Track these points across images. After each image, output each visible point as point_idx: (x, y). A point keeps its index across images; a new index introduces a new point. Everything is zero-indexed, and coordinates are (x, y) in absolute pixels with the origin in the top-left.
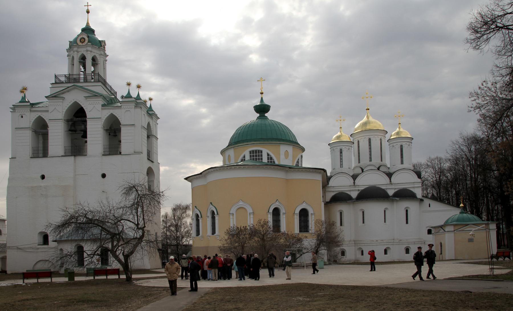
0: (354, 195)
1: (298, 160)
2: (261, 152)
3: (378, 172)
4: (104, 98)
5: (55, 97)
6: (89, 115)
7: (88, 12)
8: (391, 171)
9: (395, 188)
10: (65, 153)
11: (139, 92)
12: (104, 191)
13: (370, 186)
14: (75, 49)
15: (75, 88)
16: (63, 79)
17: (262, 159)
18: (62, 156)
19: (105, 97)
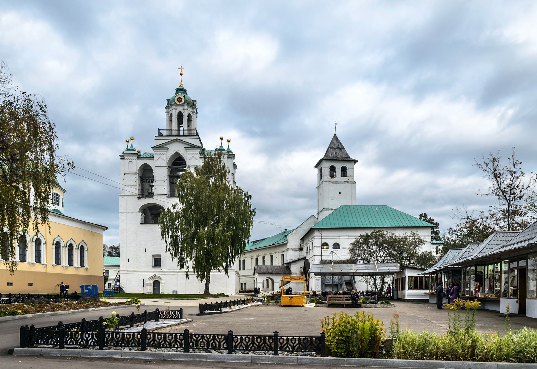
7: (181, 74)
14: (174, 107)
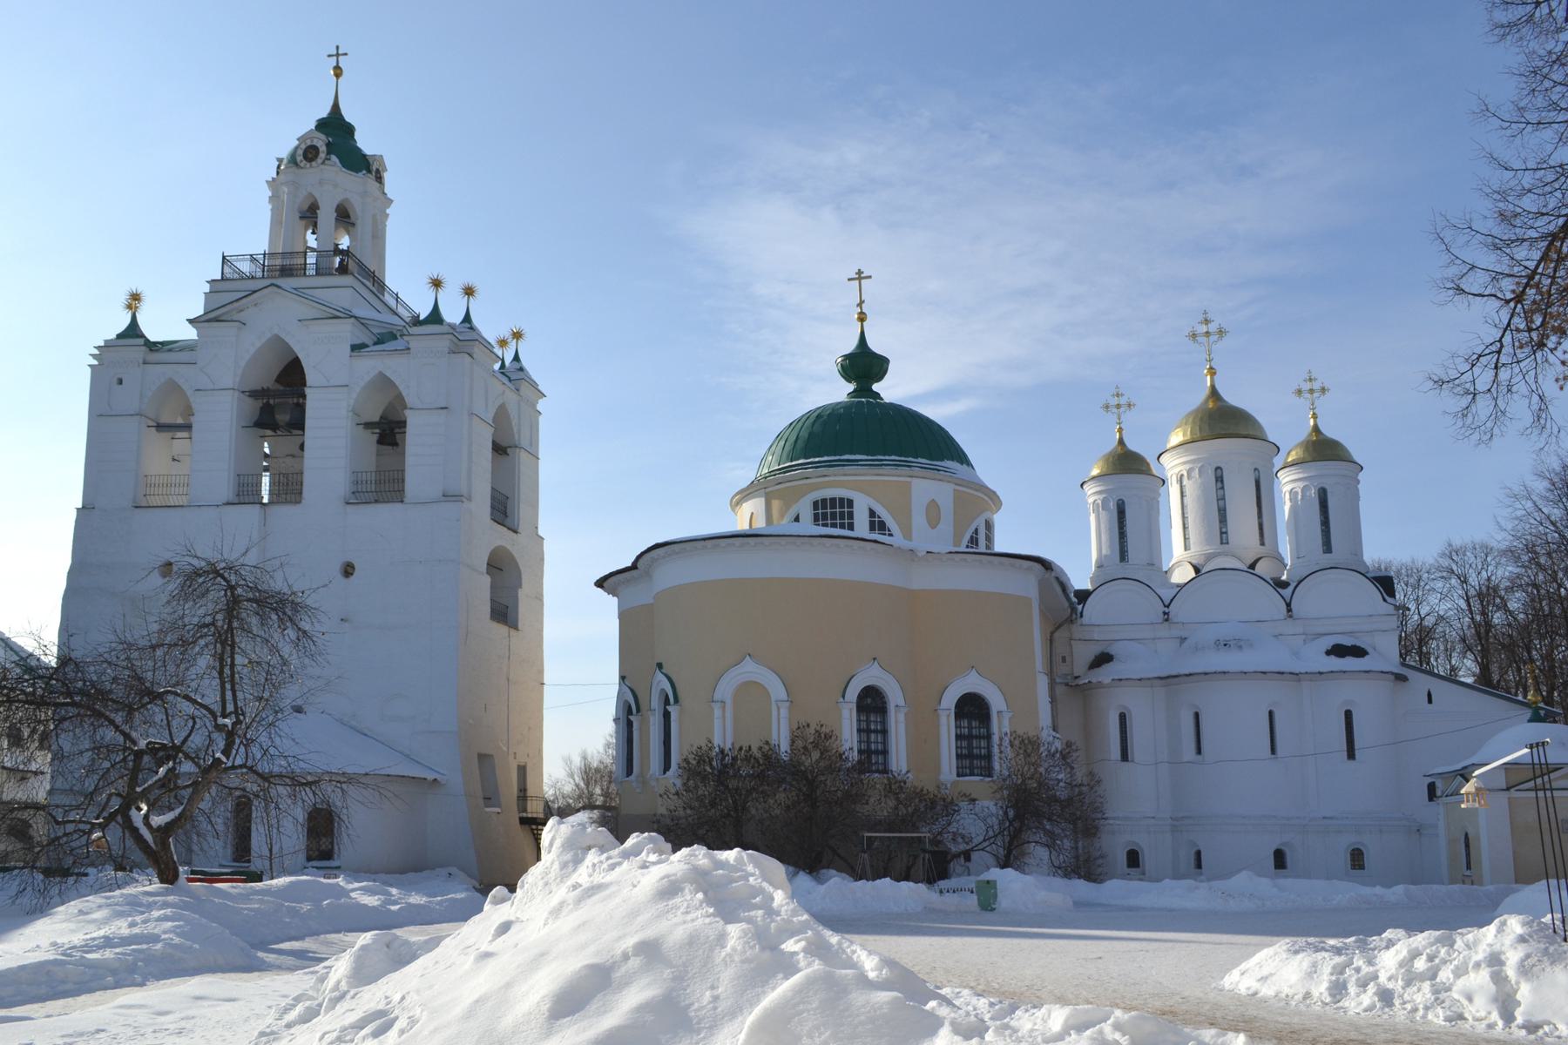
5: (217, 320)
6: (311, 377)
10: (238, 495)
12: (343, 618)
16: (246, 267)
19: (362, 321)
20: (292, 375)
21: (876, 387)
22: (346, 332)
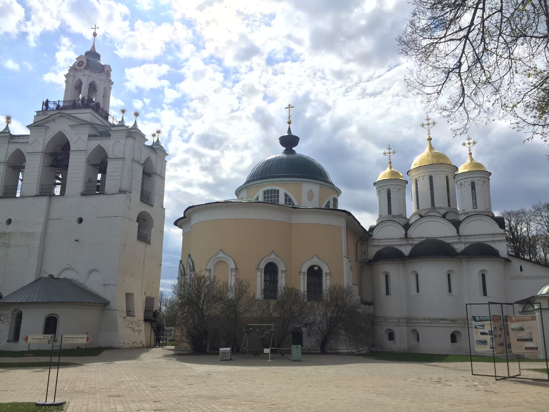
0: (406, 250)
1: (329, 202)
2: (278, 191)
3: (443, 221)
4: (91, 125)
6: (72, 147)
8: (461, 218)
9: (465, 242)
11: (136, 121)
13: (426, 239)
15: (62, 116)
17: (278, 201)
18: (36, 196)
20: (66, 147)
21: (294, 149)
22: (87, 130)
